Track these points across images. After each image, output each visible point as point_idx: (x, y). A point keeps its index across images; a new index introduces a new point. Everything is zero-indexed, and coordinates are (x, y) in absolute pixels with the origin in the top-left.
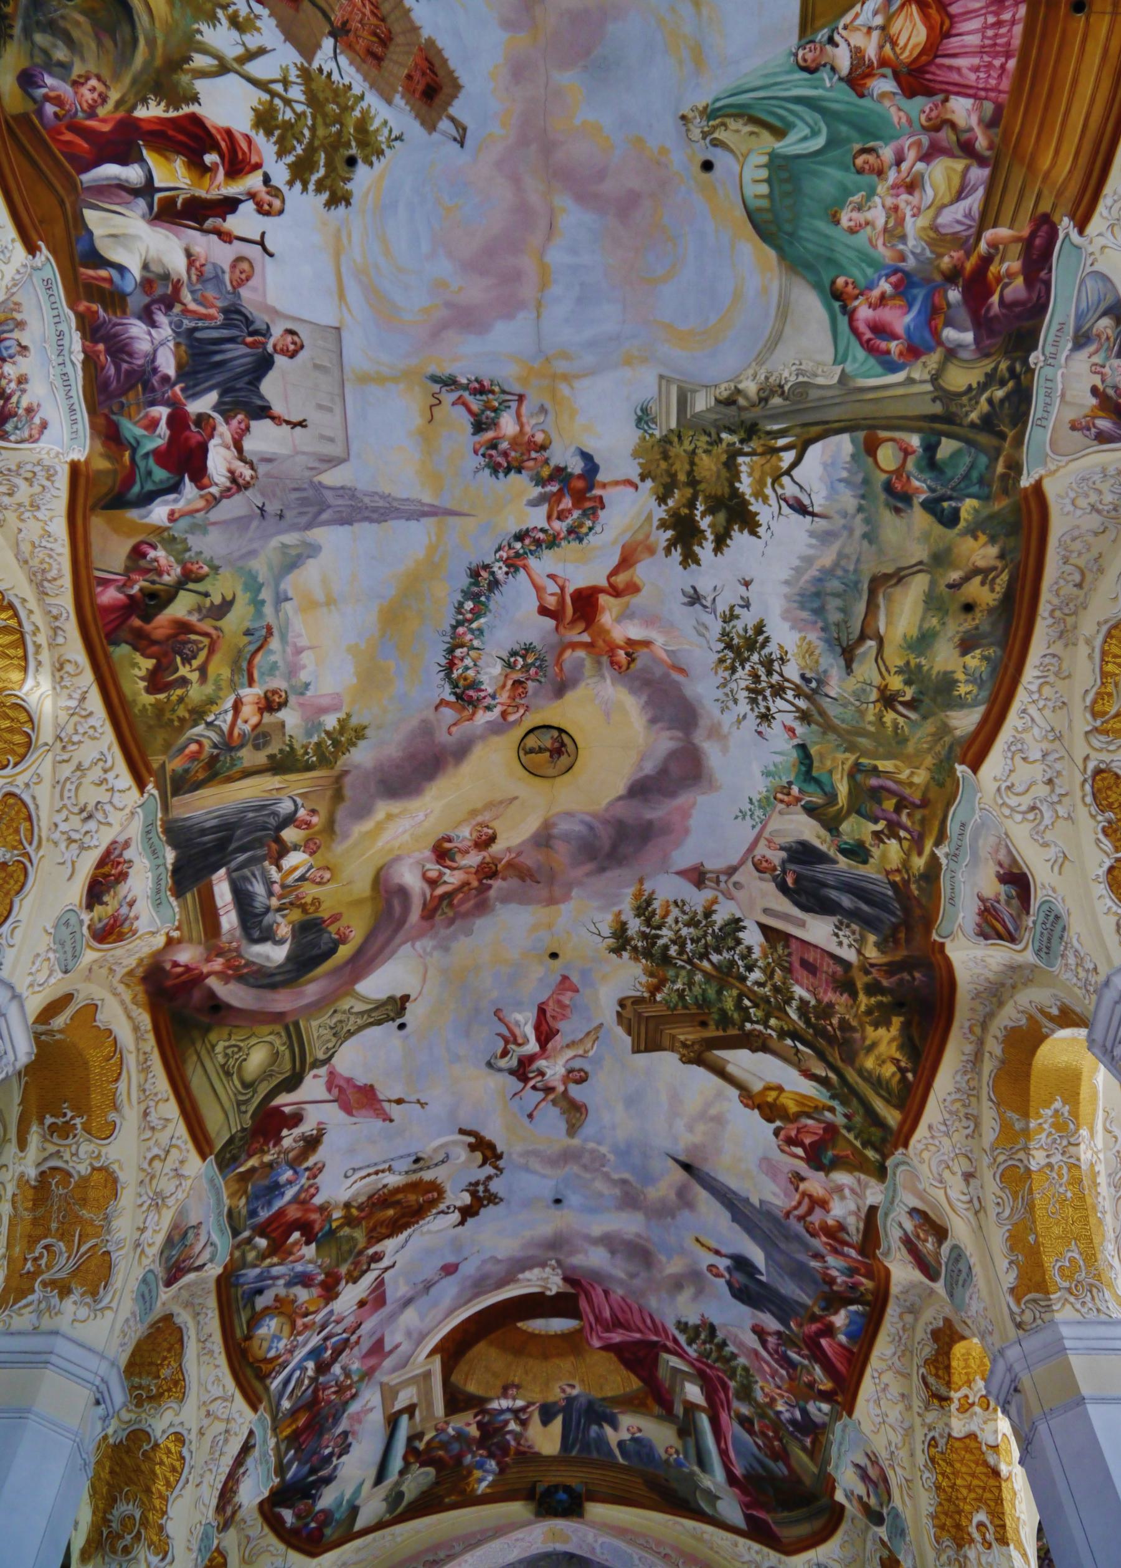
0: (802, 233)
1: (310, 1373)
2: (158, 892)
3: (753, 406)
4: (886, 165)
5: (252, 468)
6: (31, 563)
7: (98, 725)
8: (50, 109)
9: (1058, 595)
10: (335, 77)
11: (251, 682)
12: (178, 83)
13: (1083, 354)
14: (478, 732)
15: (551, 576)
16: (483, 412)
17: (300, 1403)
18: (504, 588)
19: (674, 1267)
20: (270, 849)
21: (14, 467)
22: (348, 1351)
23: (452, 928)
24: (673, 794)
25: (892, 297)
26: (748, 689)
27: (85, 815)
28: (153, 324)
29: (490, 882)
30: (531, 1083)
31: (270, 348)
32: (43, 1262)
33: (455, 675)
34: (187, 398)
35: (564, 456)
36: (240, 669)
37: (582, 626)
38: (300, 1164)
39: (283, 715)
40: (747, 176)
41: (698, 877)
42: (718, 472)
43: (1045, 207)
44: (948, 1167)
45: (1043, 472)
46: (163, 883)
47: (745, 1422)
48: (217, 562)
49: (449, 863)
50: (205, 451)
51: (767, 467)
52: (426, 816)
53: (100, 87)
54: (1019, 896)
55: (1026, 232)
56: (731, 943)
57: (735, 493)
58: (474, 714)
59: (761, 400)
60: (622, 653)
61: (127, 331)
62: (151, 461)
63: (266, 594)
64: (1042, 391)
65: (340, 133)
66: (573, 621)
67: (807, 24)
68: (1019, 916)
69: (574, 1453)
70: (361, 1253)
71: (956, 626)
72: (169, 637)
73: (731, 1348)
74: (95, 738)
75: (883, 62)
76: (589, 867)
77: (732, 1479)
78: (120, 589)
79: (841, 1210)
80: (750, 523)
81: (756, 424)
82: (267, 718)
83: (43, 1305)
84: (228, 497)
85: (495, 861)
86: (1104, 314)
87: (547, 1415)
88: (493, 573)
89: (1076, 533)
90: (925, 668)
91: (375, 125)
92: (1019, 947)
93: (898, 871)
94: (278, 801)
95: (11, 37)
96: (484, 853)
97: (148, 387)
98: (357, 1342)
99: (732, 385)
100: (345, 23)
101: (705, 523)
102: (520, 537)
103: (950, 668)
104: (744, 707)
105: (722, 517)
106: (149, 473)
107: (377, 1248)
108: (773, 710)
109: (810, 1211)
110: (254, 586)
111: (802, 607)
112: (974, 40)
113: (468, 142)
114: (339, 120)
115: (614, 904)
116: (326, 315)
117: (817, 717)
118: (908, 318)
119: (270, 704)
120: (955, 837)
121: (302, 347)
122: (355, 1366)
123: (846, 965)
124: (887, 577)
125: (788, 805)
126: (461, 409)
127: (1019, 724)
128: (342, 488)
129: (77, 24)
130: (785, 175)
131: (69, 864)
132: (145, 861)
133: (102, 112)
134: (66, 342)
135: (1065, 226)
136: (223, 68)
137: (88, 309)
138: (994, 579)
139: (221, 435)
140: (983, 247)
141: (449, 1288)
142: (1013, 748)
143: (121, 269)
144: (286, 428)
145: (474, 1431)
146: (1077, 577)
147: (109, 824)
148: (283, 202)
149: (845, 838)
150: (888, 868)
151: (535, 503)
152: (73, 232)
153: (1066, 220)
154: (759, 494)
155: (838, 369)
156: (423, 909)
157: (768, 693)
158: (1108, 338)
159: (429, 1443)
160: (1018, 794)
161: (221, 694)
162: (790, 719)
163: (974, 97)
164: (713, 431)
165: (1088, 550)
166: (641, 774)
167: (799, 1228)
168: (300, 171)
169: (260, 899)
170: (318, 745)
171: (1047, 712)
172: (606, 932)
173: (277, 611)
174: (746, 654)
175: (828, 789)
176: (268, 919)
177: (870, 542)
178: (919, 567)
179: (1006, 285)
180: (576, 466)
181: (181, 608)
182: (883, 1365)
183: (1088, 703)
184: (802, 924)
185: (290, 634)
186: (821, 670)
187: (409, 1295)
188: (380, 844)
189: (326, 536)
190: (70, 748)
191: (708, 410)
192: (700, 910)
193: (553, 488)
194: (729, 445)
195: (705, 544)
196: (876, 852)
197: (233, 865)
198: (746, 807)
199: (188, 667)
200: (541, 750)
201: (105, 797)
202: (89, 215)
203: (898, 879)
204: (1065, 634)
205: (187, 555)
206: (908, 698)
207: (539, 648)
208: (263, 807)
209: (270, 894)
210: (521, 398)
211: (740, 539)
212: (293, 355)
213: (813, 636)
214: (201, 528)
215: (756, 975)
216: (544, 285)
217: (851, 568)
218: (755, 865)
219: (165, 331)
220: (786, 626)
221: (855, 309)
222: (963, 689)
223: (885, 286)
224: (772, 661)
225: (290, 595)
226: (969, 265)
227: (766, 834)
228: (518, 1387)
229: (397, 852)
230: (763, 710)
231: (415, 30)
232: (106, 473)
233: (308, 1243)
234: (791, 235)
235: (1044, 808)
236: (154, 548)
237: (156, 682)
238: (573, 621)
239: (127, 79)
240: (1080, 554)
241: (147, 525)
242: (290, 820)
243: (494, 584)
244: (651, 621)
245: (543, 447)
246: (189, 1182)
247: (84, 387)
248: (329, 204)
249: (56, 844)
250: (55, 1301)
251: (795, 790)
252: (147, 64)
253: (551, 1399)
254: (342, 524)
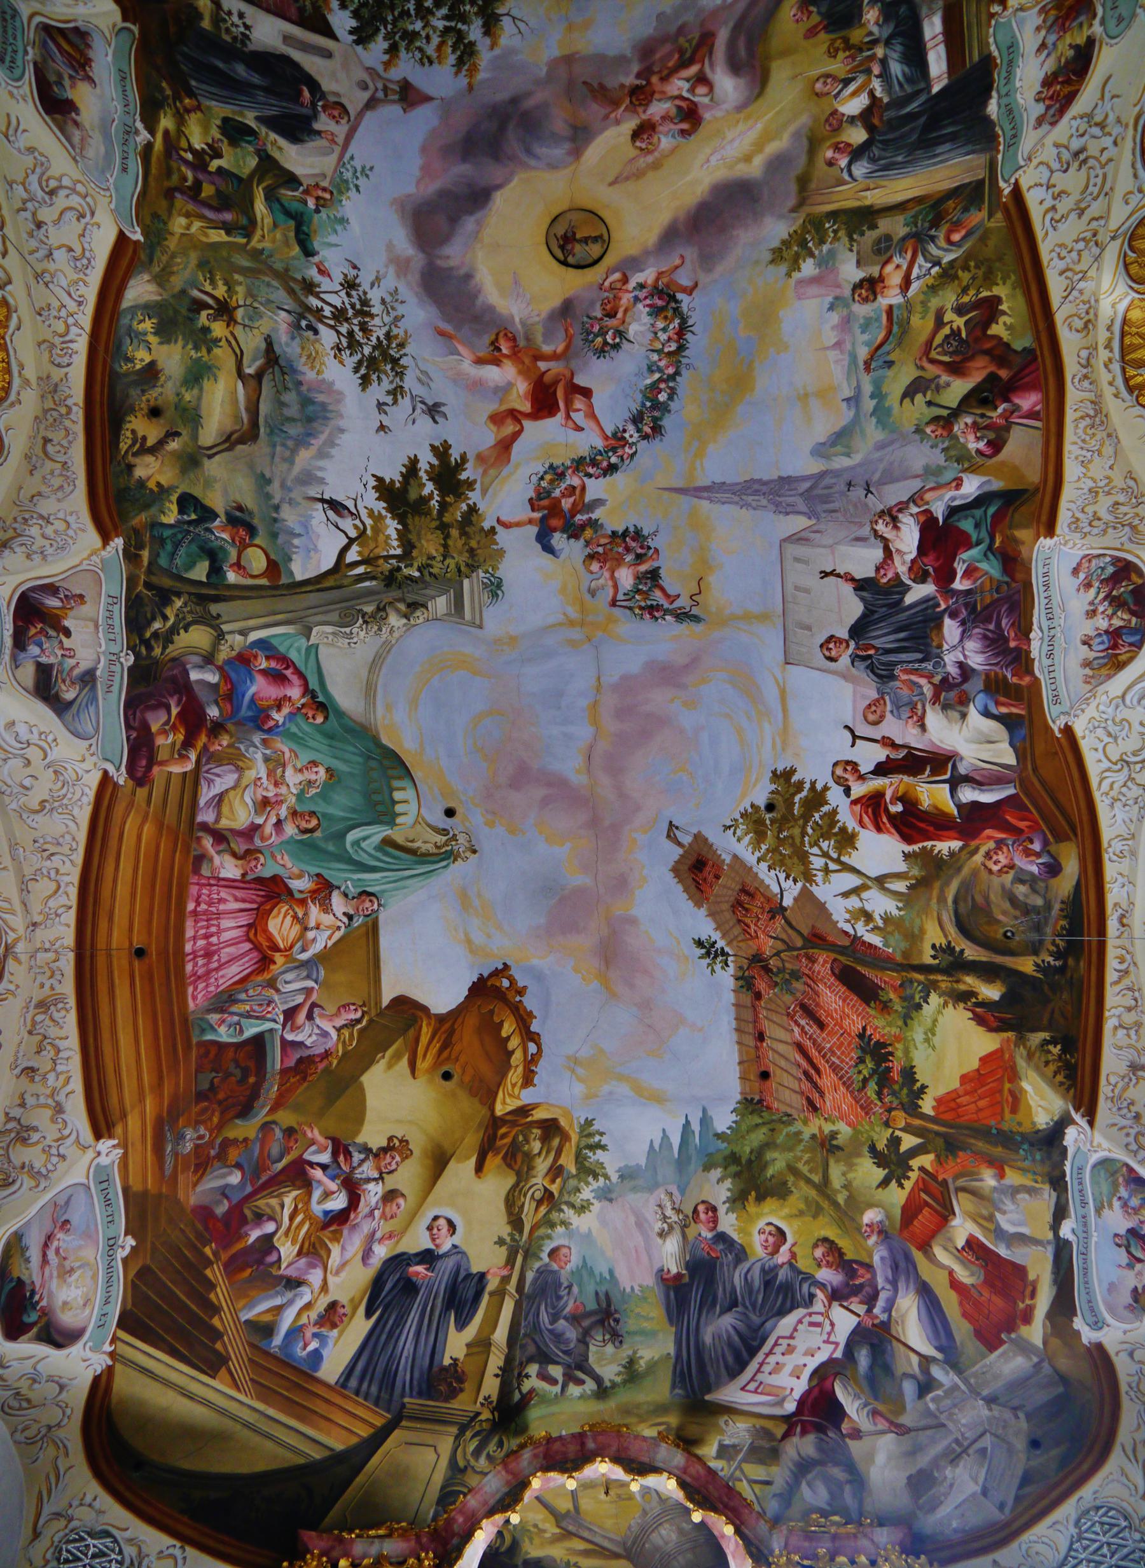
0: (360, 760)
2: (1011, 63)
3: (390, 603)
4: (290, 818)
5: (875, 531)
6: (1104, 434)
7: (1056, 260)
8: (1037, 846)
9: (66, 429)
10: (782, 876)
11: (890, 310)
12: (921, 869)
13: (84, 666)
14: (652, 260)
15: (579, 429)
16: (650, 589)
18: (627, 415)
20: (881, 119)
21: (1110, 530)
23: (680, 22)
24: (443, 194)
25: (270, 707)
26: (372, 316)
27: (1082, 157)
28: (961, 665)
29: (638, 82)
31: (852, 644)
33: (677, 321)
34: (934, 598)
35: (571, 550)
36: (900, 325)
37: (547, 378)
39: (858, 275)
40: (413, 807)
42: (419, 539)
43: (142, 793)
45: (103, 553)
46: (1004, 74)
48: (917, 437)
49: (683, 104)
50: (920, 548)
51: (372, 545)
52: (708, 161)
53: (990, 864)
54: (49, 85)
55: (156, 770)
56: (365, 12)
57: (401, 519)
58: (657, 279)
59: (384, 609)
60: (505, 351)
61: (988, 658)
62: (974, 538)
63: (869, 405)
64: (117, 629)
65: (780, 831)
66: (556, 382)
67: (372, 930)
68: (44, 60)
71: (166, 391)
72: (972, 358)
74: (1060, 246)
75: (302, 902)
76: (529, 103)
78: (1018, 408)
80: (384, 489)
81: (387, 586)
82: (875, 271)
84: (900, 503)
85: (632, 109)
86: (71, 703)
88: (639, 430)
89: (60, 494)
90: (190, 346)
91: (747, 839)
92: (38, 19)
93: (188, 111)
94: (868, 176)
95: (1063, 902)
96: (644, 117)
97: (971, 608)
99: (412, 622)
100: (773, 917)
101: (429, 487)
102: (612, 469)
103: (165, 347)
104: (374, 296)
105: (413, 495)
106: (977, 526)
108: (343, 294)
110: (881, 413)
111: (324, 406)
112: (226, 923)
113: (666, 826)
114: (781, 842)
115: (497, 57)
116: (797, 675)
117: (297, 288)
118: (253, 690)
119: (871, 287)
120: (132, 156)
121: (821, 646)
124: (242, 441)
125: (317, 186)
126: (671, 591)
127: (83, 290)
128: (787, 514)
129: (1004, 913)
130: (380, 808)
131: (1107, 96)
132: (1021, 101)
133: (991, 845)
134: (1045, 648)
135: (121, 777)
136: (880, 881)
137: (1021, 678)
138: (134, 444)
139: (904, 563)
140: (193, 756)
142: (85, 262)
143: (987, 714)
144: (841, 570)
146: (50, 448)
147: (1057, 145)
148: (833, 773)
149: (251, 149)
150: (199, 114)
151: (598, 503)
152: (1028, 745)
153: (121, 782)
154: (378, 519)
155: (313, 640)
156: (713, 45)
157: (350, 312)
158: (64, 681)
160: (71, 208)
161: (922, 297)
162: (325, 284)
163: (219, 879)
164: (427, 578)
165: (44, 478)
166: (479, 215)
168: (817, 798)
169: (895, 56)
170: (822, 242)
171: (56, 304)
172: (506, 22)
173: (858, 388)
174: (377, 353)
175: (276, 206)
176: (887, 31)
177: (263, 475)
178: (211, 452)
179: (167, 723)
180: (558, 540)
181: (957, 389)
183: (14, 315)
184: (287, 39)
185: (846, 363)
186: (298, 340)
188: (759, 126)
189: (806, 465)
190: (1088, 235)
191: (433, 598)
192: (403, 53)
193: (580, 518)
194: (411, 565)
195: (427, 467)
196: (215, 133)
197: (923, 98)
198: (362, 182)
199: (955, 326)
200: (585, 240)
201: (1058, 178)
202: (1010, 759)
203: (187, 101)
204: (51, 389)
205: (946, 444)
206: (204, 314)
207: (590, 354)
208: (886, 168)
209: (884, 62)
210: (614, 603)
211: (393, 473)
212: (831, 638)
213: (310, 375)
214: (930, 471)
216: (595, 704)
217: (278, 448)
218: (347, 112)
219: (950, 660)
220: (338, 386)
221: (303, 696)
222: (148, 325)
223: (278, 717)
224: (349, 347)
225: (844, 404)
226: (203, 739)
227: (338, 149)
229: (742, 115)
230: (354, 293)
231: (711, 914)
232: (1020, 526)
234: (369, 758)
235: (40, 194)
236: (978, 451)
237: (990, 309)
238: (556, 382)
239: (966, 871)
240: (52, 473)
241: (984, 475)
242: (857, 153)
243: (637, 420)
244: (476, 386)
245: (591, 557)
247: (1033, 607)
248: (793, 771)
249: (1119, 121)
251: (311, 203)
252: (947, 883)
254: (789, 477)
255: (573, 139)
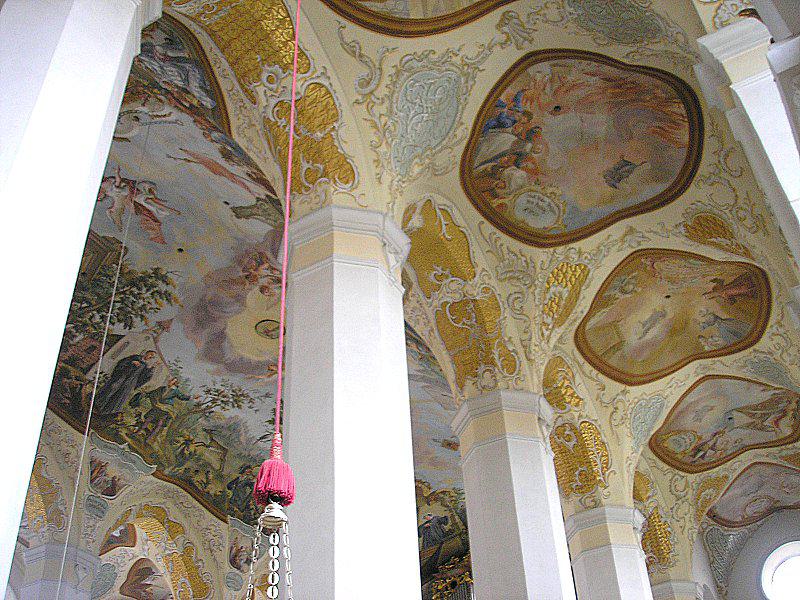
30: (118, 180)
41: (163, 326)
56: (121, 317)
76: (209, 298)
104: (218, 387)
123: (86, 371)
192: (147, 315)
196: (133, 411)
204: (167, 494)
213: (223, 422)
215: (97, 319)
251: (174, 387)
255: (238, 301)
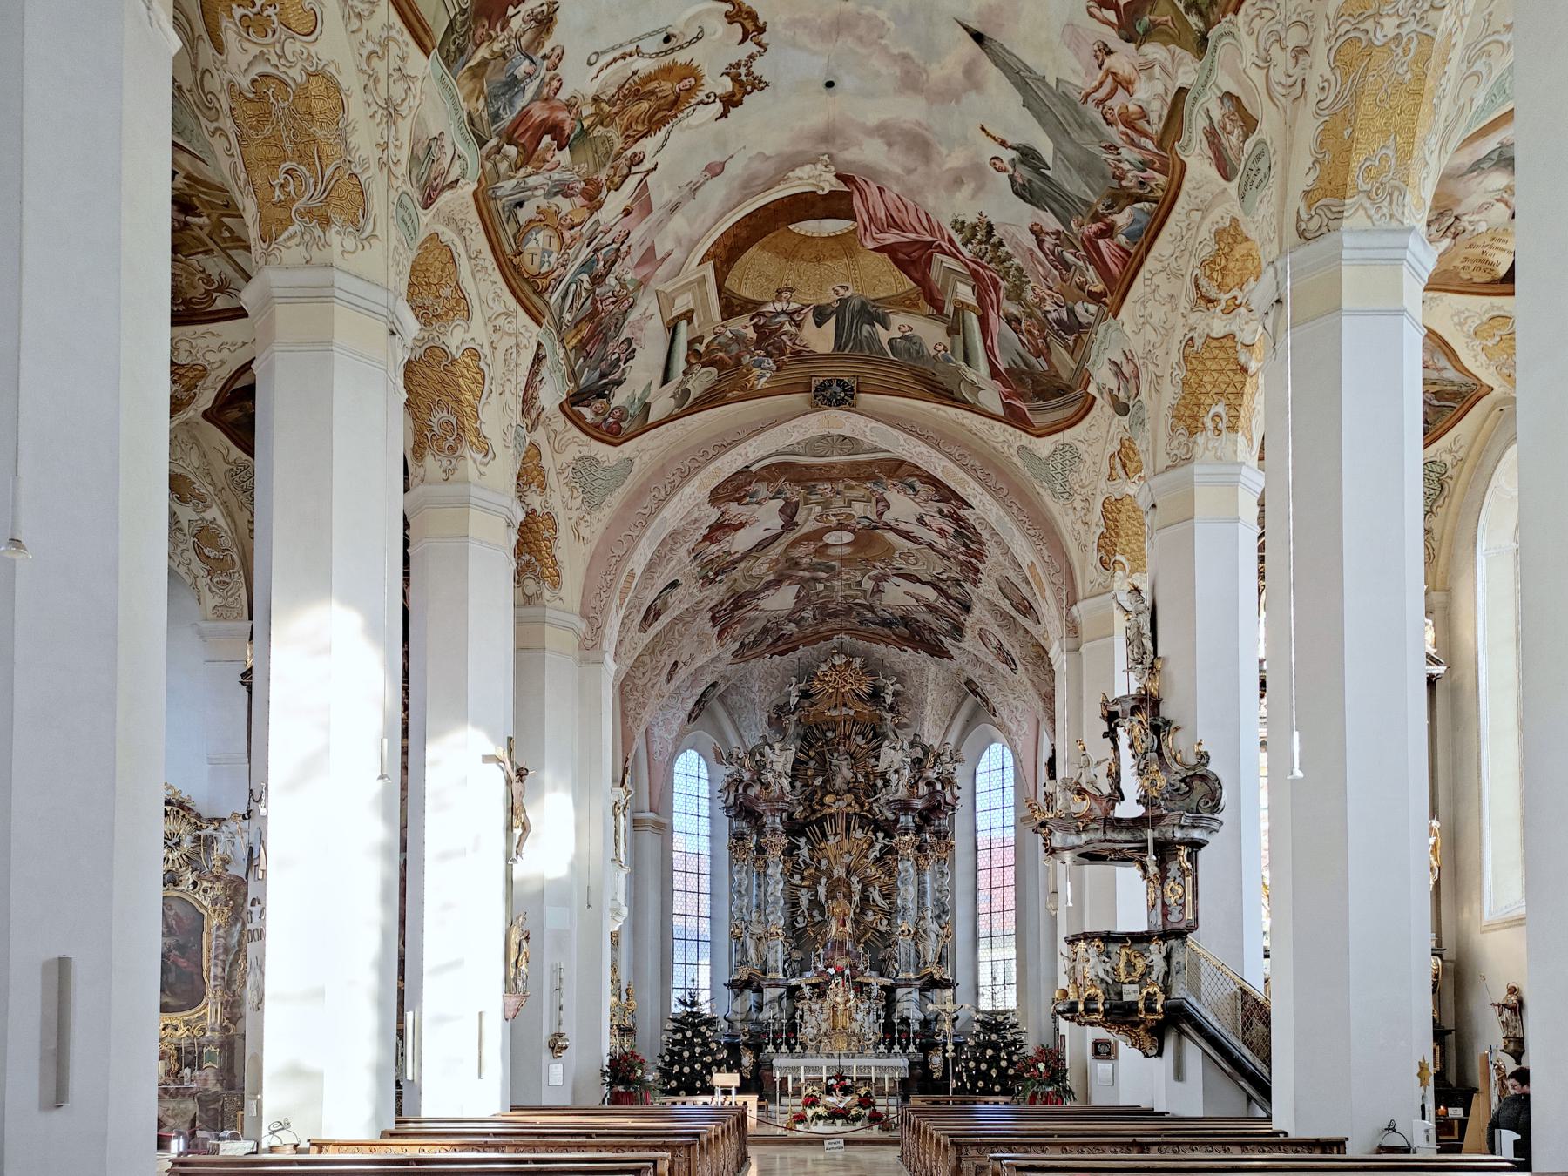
1: (586, 285)
17: (581, 315)
19: (955, 160)
22: (620, 261)
32: (291, 188)
38: (536, 51)
44: (1279, 40)
47: (1012, 321)
69: (846, 352)
70: (619, 155)
73: (1007, 248)
77: (995, 373)
79: (1149, 95)
83: (307, 237)
87: (821, 316)
98: (628, 253)
107: (636, 148)
109: (1112, 93)
122: (628, 277)
141: (716, 191)
145: (751, 334)
159: (708, 346)
167: (1094, 113)
182: (1159, 266)
187: (674, 200)
228: (791, 290)
233: (560, 148)
246: (418, 84)
250: (318, 232)
253: (825, 302)
